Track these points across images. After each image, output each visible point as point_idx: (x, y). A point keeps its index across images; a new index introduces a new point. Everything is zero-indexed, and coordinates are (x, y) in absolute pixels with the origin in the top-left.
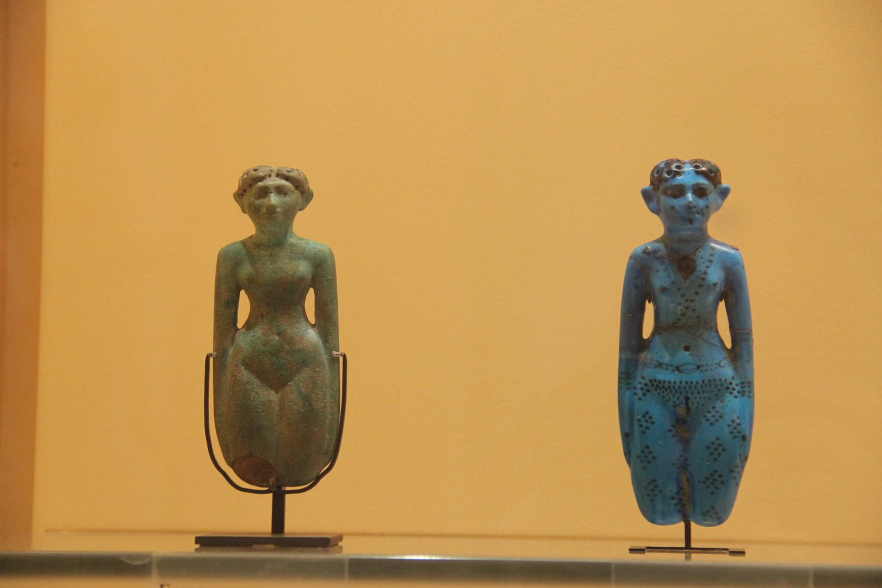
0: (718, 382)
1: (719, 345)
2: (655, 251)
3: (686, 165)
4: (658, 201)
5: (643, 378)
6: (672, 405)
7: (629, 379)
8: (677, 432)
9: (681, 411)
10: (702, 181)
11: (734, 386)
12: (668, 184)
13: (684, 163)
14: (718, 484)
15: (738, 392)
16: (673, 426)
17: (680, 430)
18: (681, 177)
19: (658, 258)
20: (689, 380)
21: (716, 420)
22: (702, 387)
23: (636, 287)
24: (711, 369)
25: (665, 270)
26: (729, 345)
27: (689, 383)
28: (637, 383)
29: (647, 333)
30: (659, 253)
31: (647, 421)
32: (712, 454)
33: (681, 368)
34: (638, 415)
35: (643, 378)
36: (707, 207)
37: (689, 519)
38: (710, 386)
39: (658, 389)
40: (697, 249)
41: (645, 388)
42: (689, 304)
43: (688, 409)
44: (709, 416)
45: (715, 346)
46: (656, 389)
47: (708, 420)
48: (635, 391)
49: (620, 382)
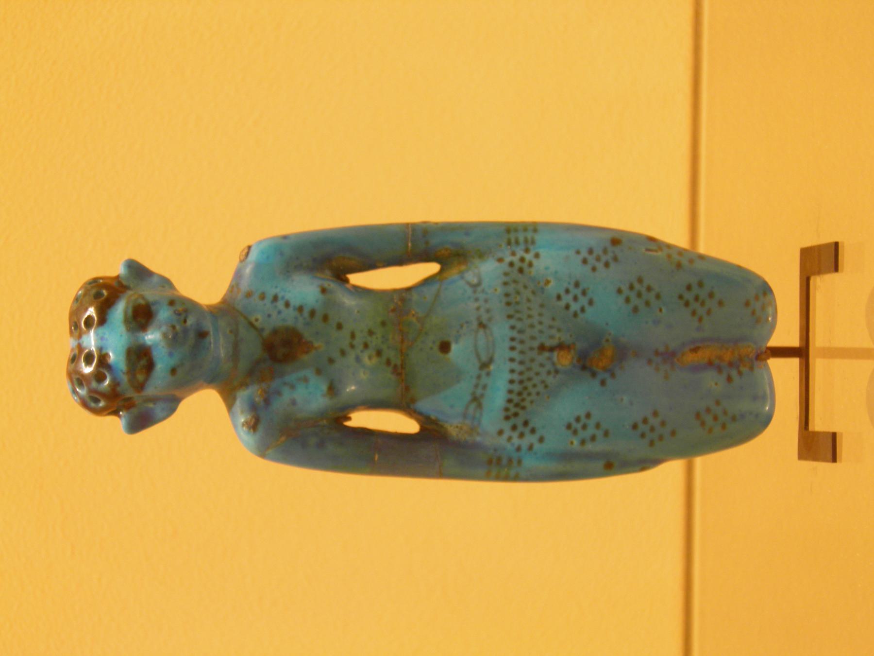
0: (511, 289)
1: (434, 288)
2: (253, 407)
3: (85, 344)
4: (154, 400)
5: (501, 432)
6: (555, 377)
7: (499, 459)
8: (605, 369)
9: (565, 360)
10: (119, 311)
11: (515, 259)
12: (124, 379)
13: (80, 348)
14: (703, 294)
15: (527, 251)
16: (594, 375)
17: (601, 364)
18: (111, 354)
19: (267, 402)
20: (508, 344)
21: (584, 293)
22: (520, 319)
23: (321, 445)
24: (486, 301)
25: (293, 387)
26: (433, 268)
27: (514, 344)
28: (509, 446)
29: (408, 425)
30: (257, 399)
31: (584, 427)
32: (647, 304)
33: (484, 358)
34: (572, 443)
35: (501, 432)
36: (172, 303)
37: (764, 349)
38: (517, 303)
39: (523, 404)
40: (251, 325)
41: (520, 428)
42: (358, 341)
43: (561, 347)
44: (575, 307)
45: (437, 296)
46: (523, 408)
47: (583, 310)
48: (524, 447)
49: (507, 478)
